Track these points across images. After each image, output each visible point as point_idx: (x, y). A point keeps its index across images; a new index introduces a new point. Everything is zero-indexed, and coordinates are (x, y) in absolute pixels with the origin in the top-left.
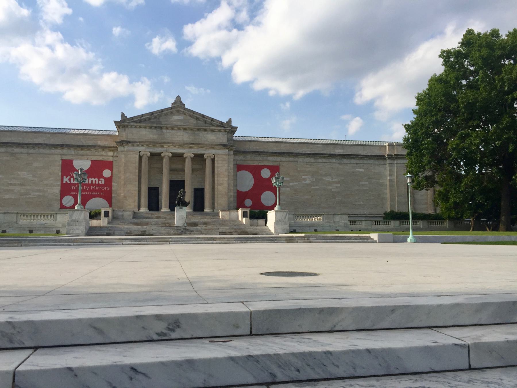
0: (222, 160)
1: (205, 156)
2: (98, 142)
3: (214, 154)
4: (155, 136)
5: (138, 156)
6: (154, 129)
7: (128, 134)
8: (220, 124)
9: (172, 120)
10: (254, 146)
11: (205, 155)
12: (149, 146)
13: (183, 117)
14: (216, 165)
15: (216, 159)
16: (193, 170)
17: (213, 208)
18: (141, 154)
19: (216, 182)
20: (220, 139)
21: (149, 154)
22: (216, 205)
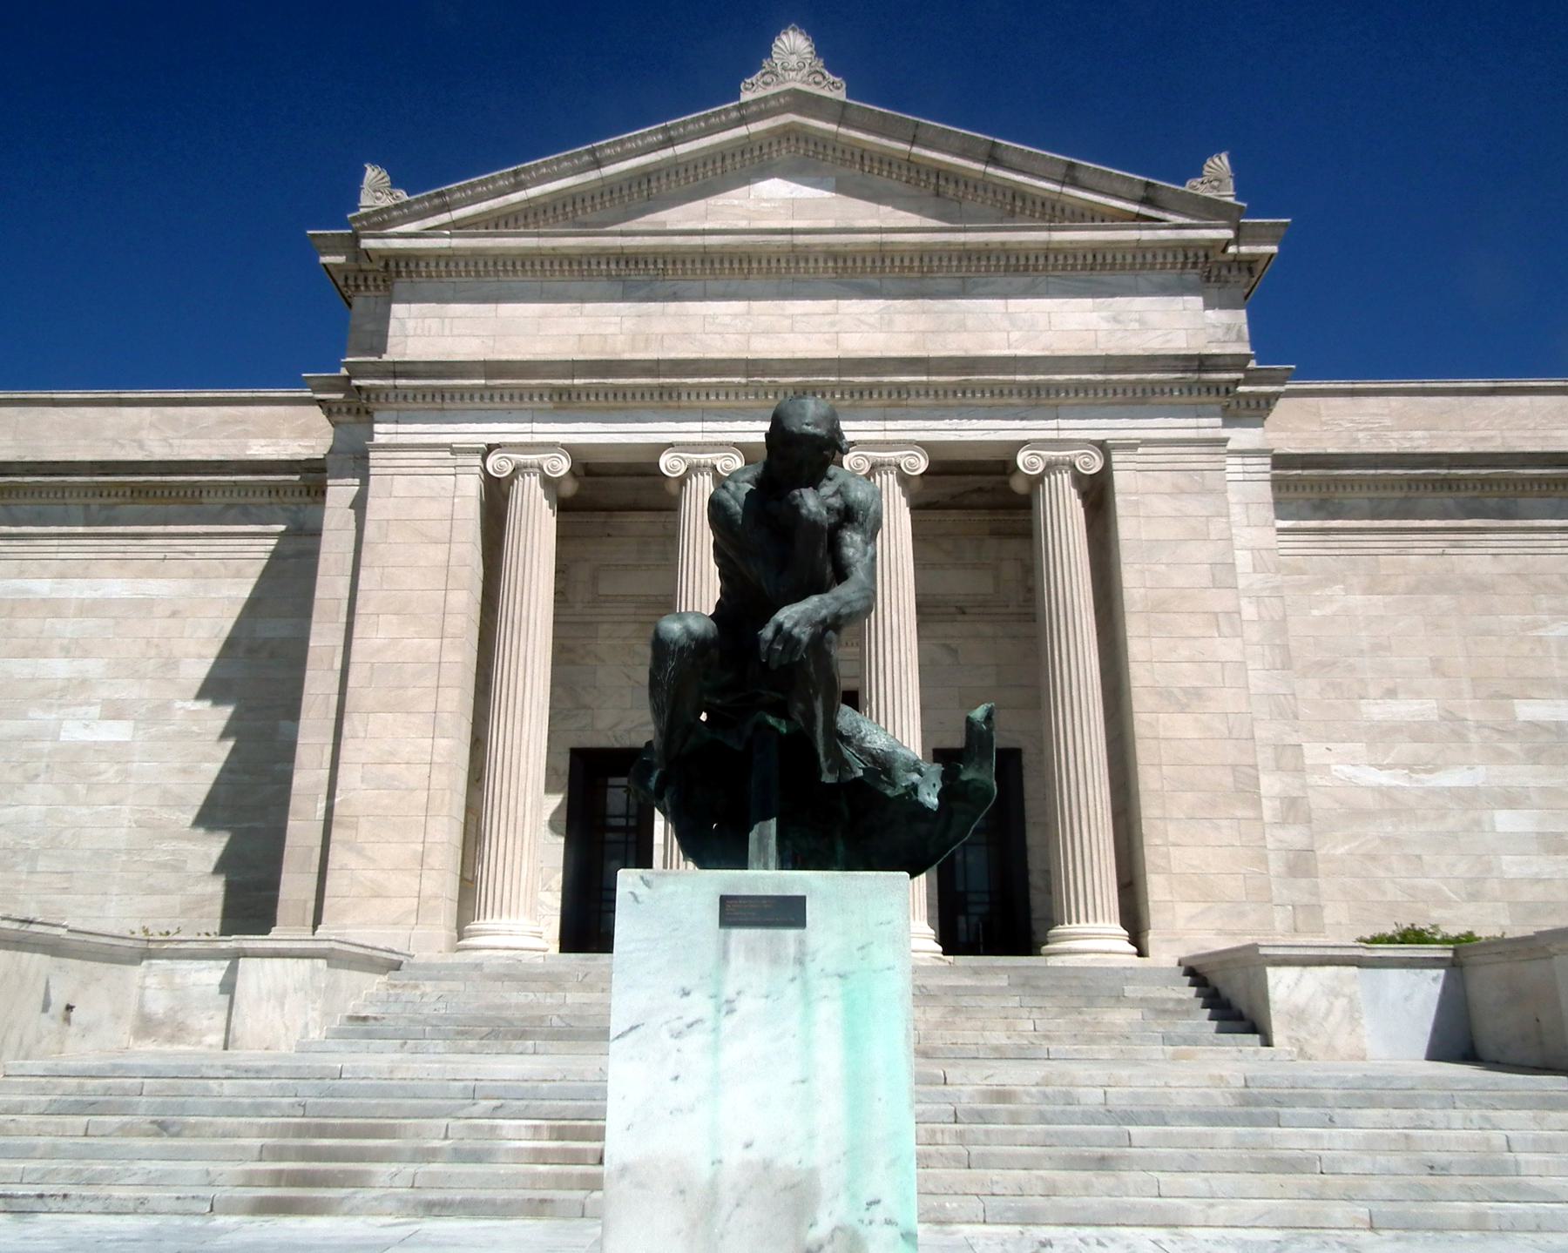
0: (1179, 492)
1: (1024, 460)
2: (252, 442)
3: (1103, 447)
4: (612, 329)
5: (471, 486)
6: (609, 276)
7: (410, 324)
8: (1135, 208)
9: (751, 205)
10: (1388, 422)
11: (1022, 458)
12: (565, 403)
13: (834, 180)
14: (1128, 528)
15: (1121, 480)
16: (928, 610)
17: (1134, 921)
18: (499, 464)
19: (1140, 675)
20: (1141, 322)
21: (561, 466)
22: (1157, 889)
